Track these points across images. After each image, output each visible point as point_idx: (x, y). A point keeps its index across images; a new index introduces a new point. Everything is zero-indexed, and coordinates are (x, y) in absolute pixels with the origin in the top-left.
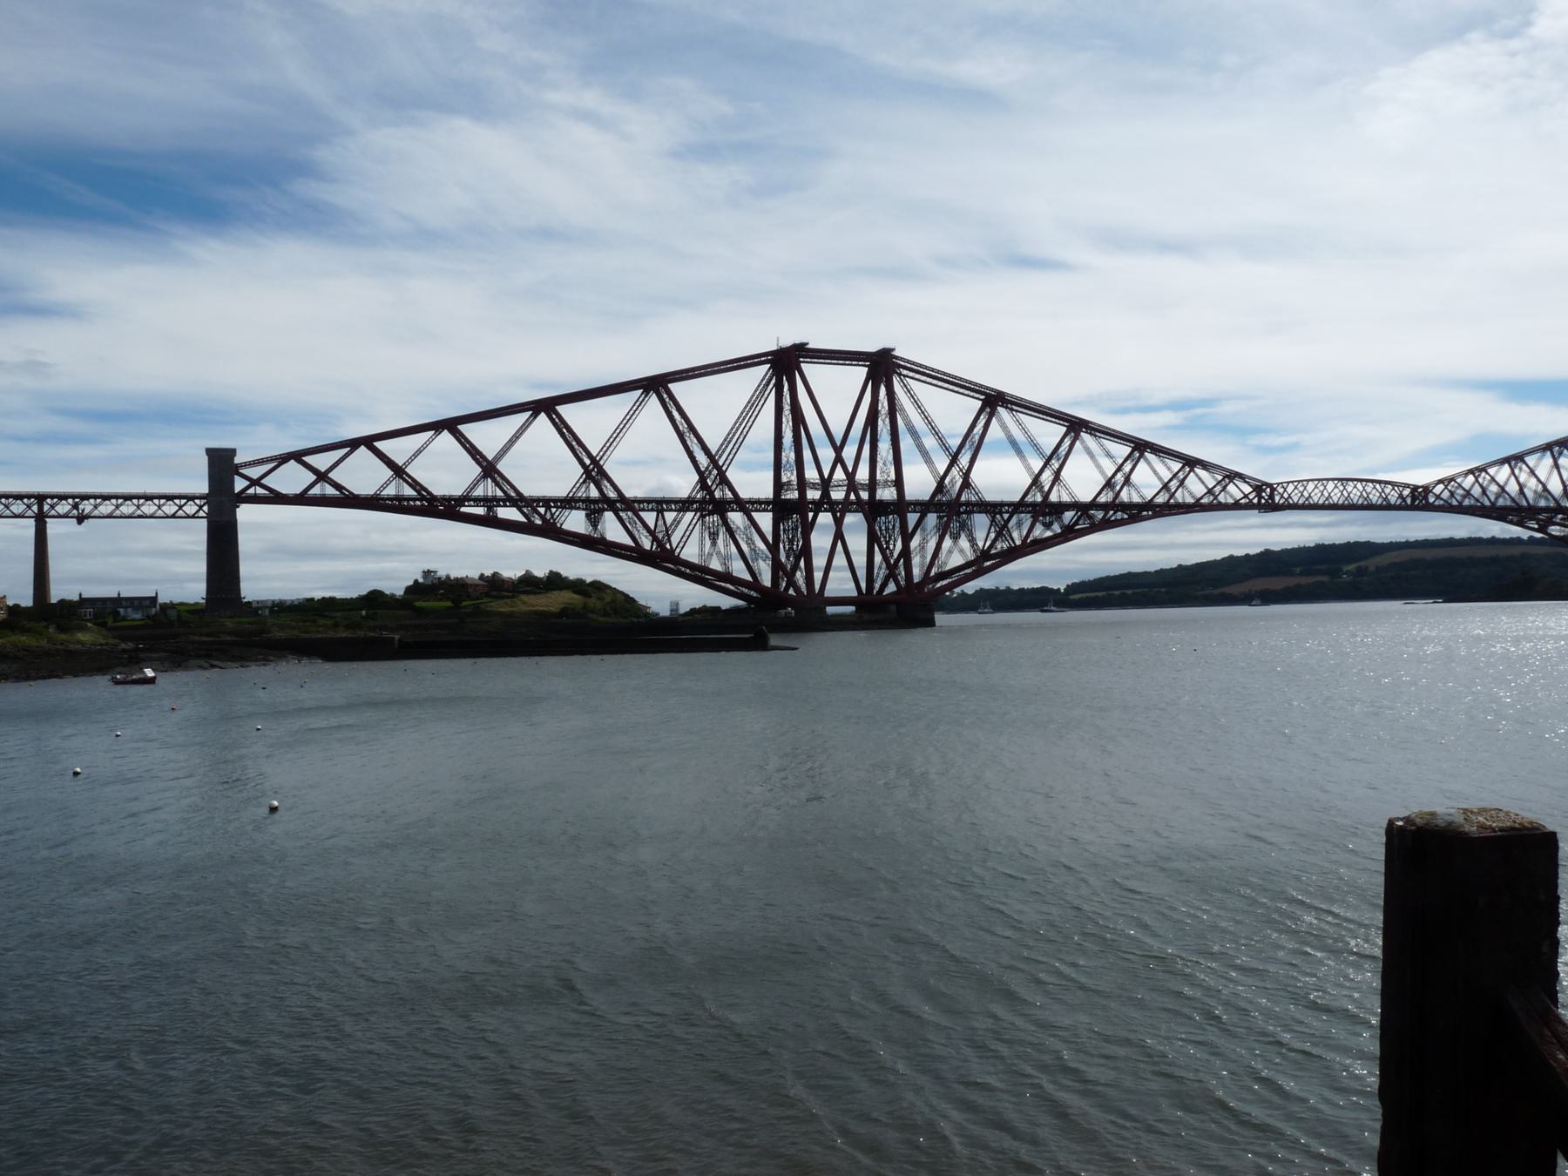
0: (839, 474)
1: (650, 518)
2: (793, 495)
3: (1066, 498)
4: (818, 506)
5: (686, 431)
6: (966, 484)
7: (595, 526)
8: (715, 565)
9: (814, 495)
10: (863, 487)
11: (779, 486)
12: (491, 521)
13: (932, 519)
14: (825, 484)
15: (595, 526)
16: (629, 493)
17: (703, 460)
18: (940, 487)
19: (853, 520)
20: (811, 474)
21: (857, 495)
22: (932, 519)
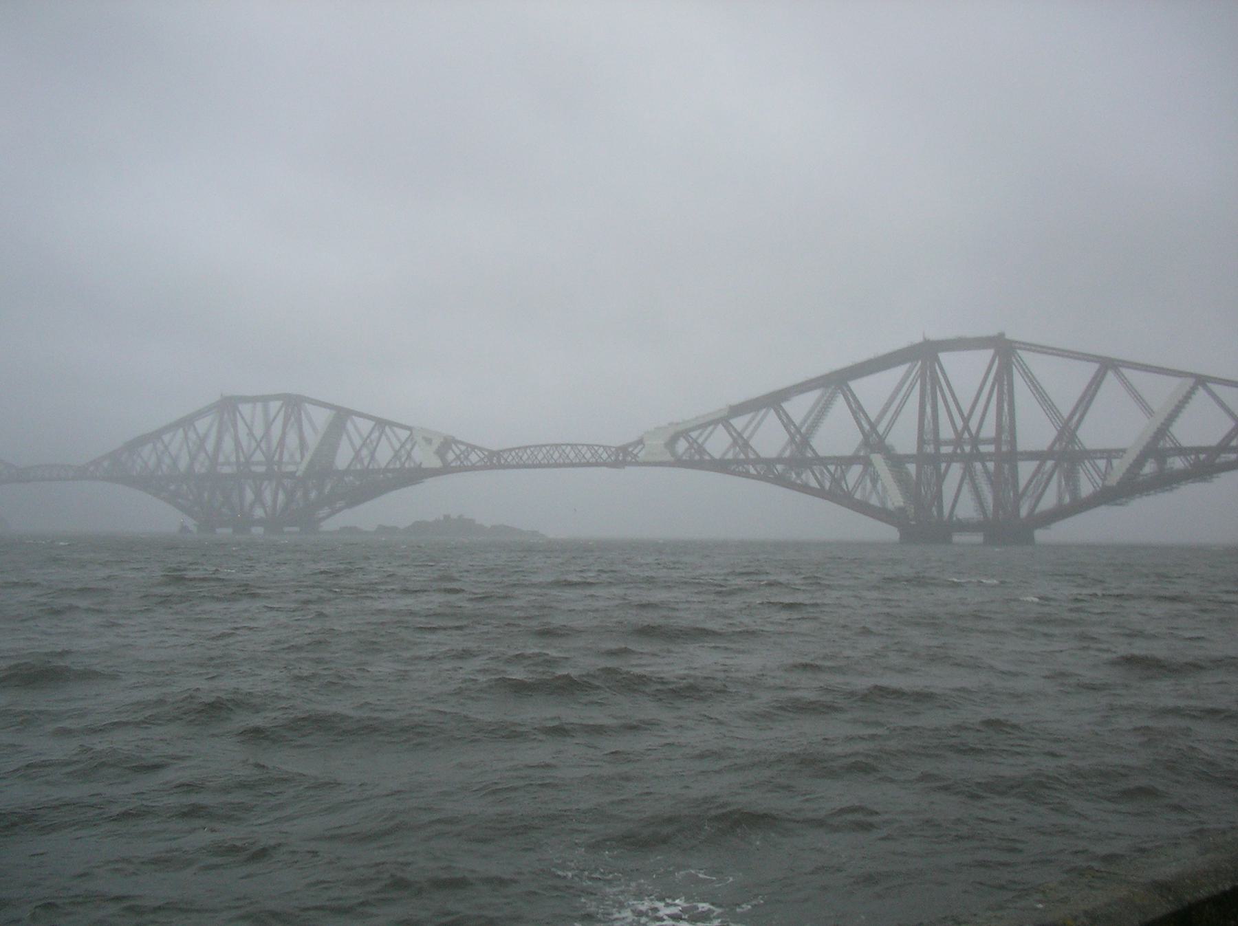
0: (966, 435)
1: (832, 468)
2: (930, 449)
3: (1169, 445)
4: (951, 458)
5: (857, 409)
6: (1073, 437)
7: (798, 475)
8: (874, 501)
9: (946, 450)
10: (987, 442)
11: (921, 441)
12: (747, 475)
13: (1049, 464)
14: (958, 441)
15: (798, 475)
16: (822, 453)
17: (867, 427)
18: (1058, 439)
19: (978, 465)
20: (946, 432)
21: (978, 450)
22: (1049, 464)
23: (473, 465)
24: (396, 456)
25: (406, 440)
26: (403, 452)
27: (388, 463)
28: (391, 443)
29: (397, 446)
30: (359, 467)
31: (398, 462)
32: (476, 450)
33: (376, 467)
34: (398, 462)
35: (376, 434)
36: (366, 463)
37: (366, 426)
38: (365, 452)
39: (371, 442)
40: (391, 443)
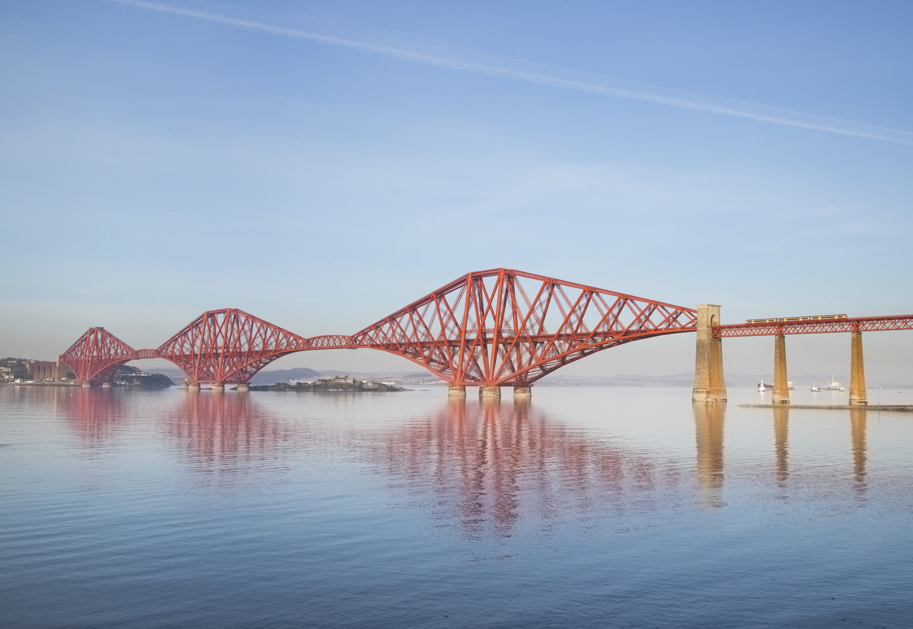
23: (656, 330)
24: (605, 319)
25: (614, 306)
26: (610, 316)
27: (597, 327)
28: (598, 308)
29: (605, 311)
30: (569, 331)
31: (606, 326)
32: (685, 312)
33: (584, 331)
34: (606, 326)
35: (583, 302)
36: (575, 327)
37: (574, 294)
38: (573, 318)
39: (580, 308)
40: (598, 308)
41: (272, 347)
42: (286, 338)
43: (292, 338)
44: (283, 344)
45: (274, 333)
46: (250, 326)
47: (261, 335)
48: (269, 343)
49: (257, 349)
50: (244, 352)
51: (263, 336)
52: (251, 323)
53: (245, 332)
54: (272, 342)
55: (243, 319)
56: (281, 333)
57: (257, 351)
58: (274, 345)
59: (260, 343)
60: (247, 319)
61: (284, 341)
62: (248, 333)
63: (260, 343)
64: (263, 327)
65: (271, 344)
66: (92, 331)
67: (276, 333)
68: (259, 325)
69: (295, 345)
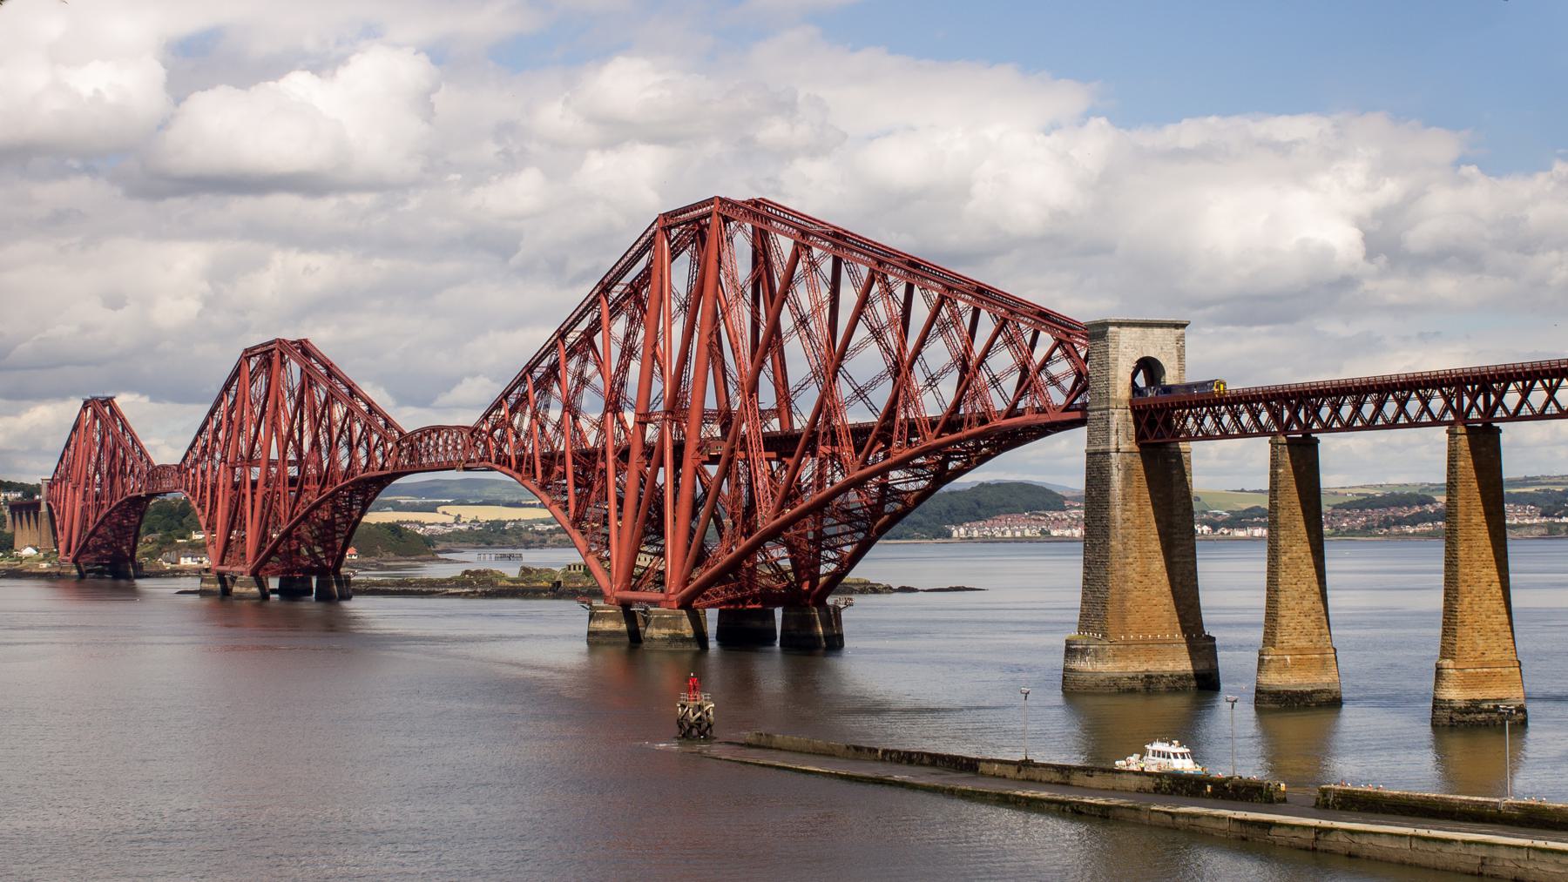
41: (933, 404)
42: (1010, 341)
43: (1046, 340)
44: (995, 381)
45: (945, 313)
46: (825, 292)
47: (877, 334)
48: (919, 378)
49: (857, 415)
50: (798, 436)
51: (891, 338)
52: (827, 266)
53: (803, 322)
54: (935, 368)
55: (784, 245)
56: (984, 313)
57: (860, 433)
58: (948, 388)
59: (873, 384)
60: (801, 249)
61: (1003, 361)
62: (819, 326)
63: (873, 384)
64: (888, 290)
65: (932, 381)
66: (269, 356)
67: (956, 317)
68: (864, 271)
69: (1068, 383)
